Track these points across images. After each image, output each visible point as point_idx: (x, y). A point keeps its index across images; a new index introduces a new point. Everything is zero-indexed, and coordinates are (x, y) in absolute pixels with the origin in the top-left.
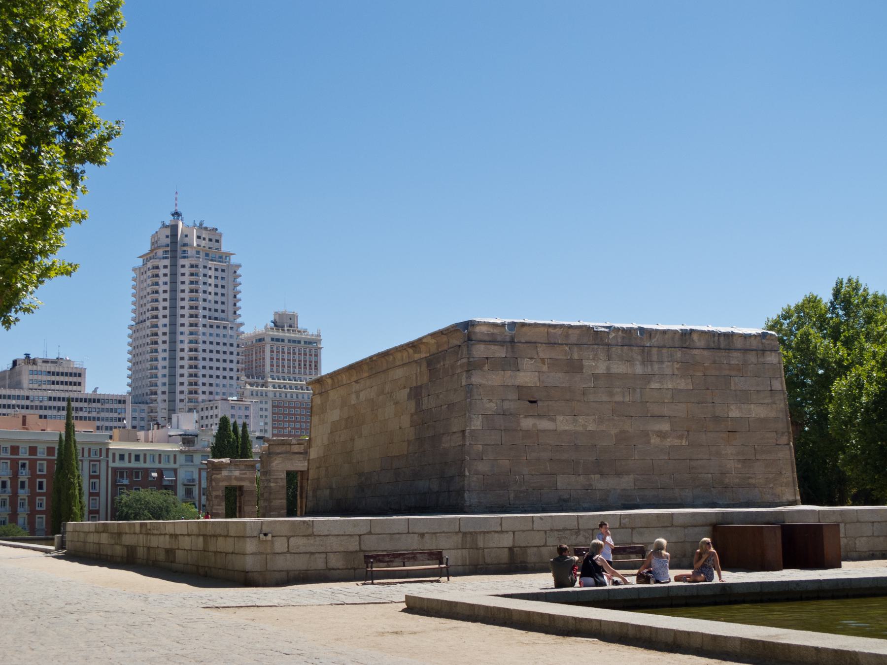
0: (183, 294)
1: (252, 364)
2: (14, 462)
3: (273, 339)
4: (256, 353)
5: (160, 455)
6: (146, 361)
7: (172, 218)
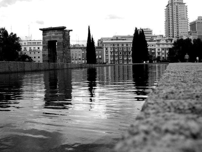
2: (114, 48)
5: (151, 45)
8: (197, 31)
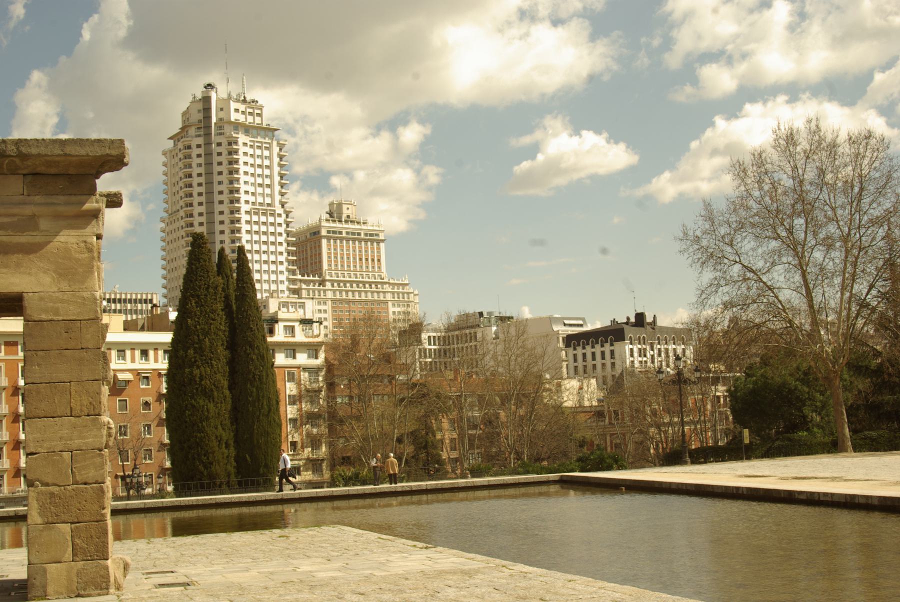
0: (220, 176)
1: (307, 262)
3: (329, 232)
4: (311, 248)
6: (181, 257)
7: (205, 89)
8: (328, 277)
